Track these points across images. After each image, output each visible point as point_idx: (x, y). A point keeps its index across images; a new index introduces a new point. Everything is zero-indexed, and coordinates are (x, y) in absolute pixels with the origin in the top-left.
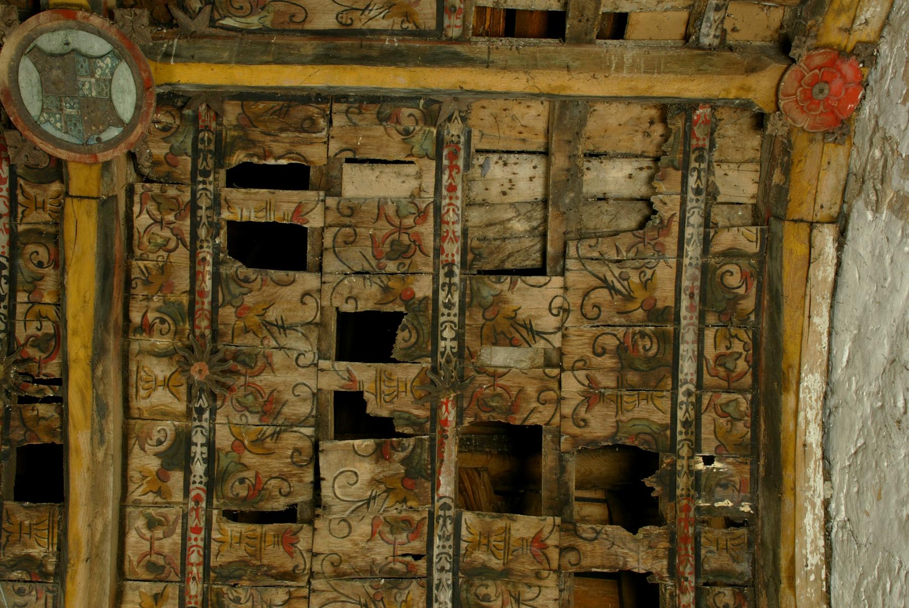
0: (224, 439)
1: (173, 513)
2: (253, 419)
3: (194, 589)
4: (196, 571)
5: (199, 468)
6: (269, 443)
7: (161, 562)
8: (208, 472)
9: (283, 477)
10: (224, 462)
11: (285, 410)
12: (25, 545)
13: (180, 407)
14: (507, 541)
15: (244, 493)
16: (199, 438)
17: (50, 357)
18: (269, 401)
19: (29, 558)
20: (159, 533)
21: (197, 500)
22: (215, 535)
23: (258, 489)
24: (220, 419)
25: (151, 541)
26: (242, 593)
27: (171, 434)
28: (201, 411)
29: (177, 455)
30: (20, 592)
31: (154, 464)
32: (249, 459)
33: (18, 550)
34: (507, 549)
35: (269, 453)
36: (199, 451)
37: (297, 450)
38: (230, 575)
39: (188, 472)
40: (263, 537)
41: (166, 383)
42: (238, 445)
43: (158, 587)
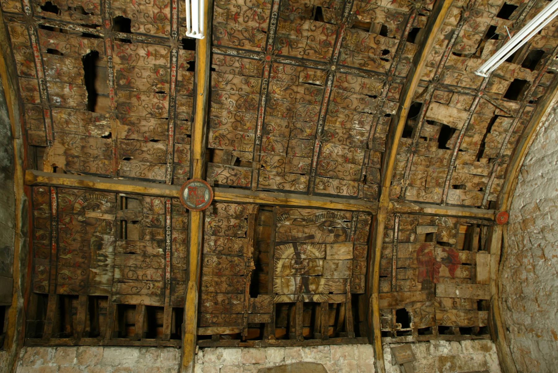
0: (462, 34)
1: (442, 51)
2: (471, 30)
3: (440, 70)
4: (442, 66)
5: (453, 40)
6: (471, 37)
7: (434, 62)
8: (454, 42)
9: (470, 46)
10: (459, 40)
11: (479, 29)
12: (408, 54)
13: (455, 23)
14: (507, 69)
15: (460, 48)
16: (456, 33)
17: (431, 4)
18: (477, 26)
19: (407, 58)
20: (436, 55)
21: (449, 49)
22: (449, 58)
23: (463, 48)
24: (463, 28)
25: (434, 57)
26: (448, 72)
27: (450, 31)
28: (460, 25)
29: (449, 37)
30: (404, 66)
31: (442, 37)
32: (465, 40)
33: (406, 55)
34: (506, 71)
35: (470, 39)
36: (455, 36)
37: (477, 40)
38: (447, 68)
39: (450, 41)
40: (458, 60)
41: (455, 16)
42: (464, 36)
43: (431, 69)
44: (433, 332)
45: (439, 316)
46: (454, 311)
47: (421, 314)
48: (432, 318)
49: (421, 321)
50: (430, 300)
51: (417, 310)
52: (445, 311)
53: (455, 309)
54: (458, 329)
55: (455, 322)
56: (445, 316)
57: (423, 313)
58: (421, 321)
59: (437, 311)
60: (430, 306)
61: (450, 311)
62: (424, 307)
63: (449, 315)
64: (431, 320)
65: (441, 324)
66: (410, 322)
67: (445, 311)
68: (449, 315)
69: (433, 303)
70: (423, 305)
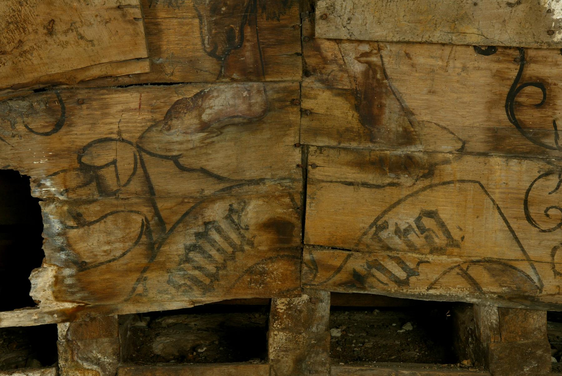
44: (277, 339)
45: (340, 208)
46: (509, 174)
47: (151, 194)
48: (277, 227)
49: (153, 250)
50: (258, 72)
51: (101, 157)
52: (407, 165)
53: (513, 154)
54: (538, 321)
55: (501, 267)
56: (405, 217)
57: (166, 181)
58: (153, 250)
59: (324, 169)
60: (251, 123)
61: (469, 167)
62: (181, 135)
63: (446, 204)
64: (264, 241)
65: (358, 278)
66: (37, 260)
67: (407, 165)
68: (446, 204)
69: (294, 98)
70: (173, 112)
